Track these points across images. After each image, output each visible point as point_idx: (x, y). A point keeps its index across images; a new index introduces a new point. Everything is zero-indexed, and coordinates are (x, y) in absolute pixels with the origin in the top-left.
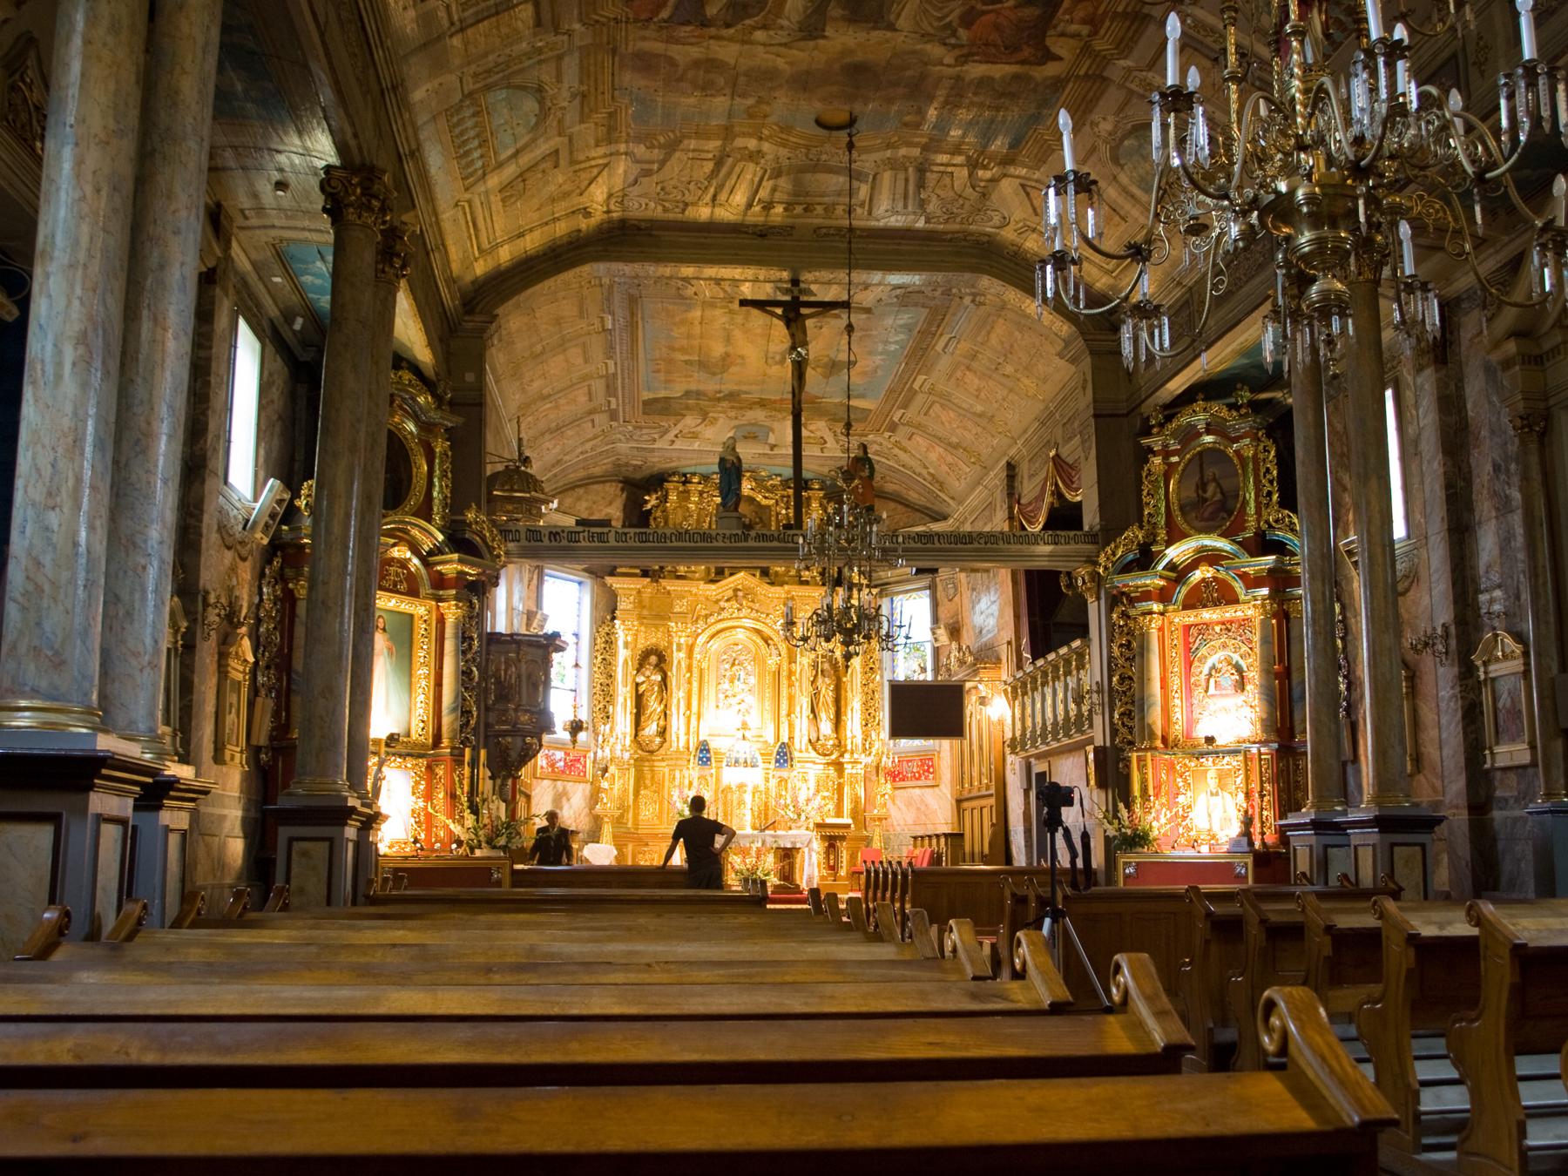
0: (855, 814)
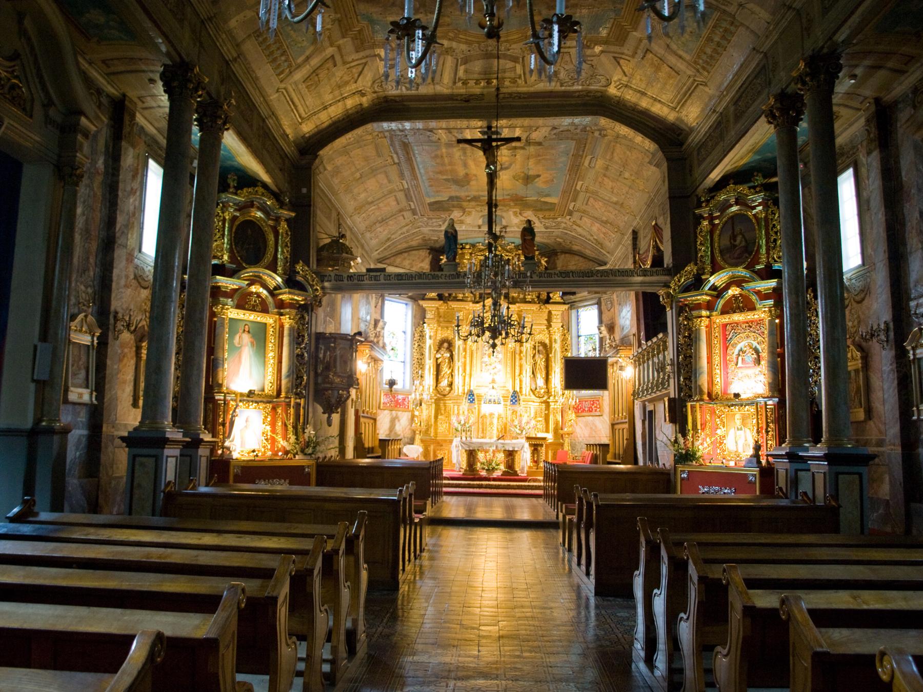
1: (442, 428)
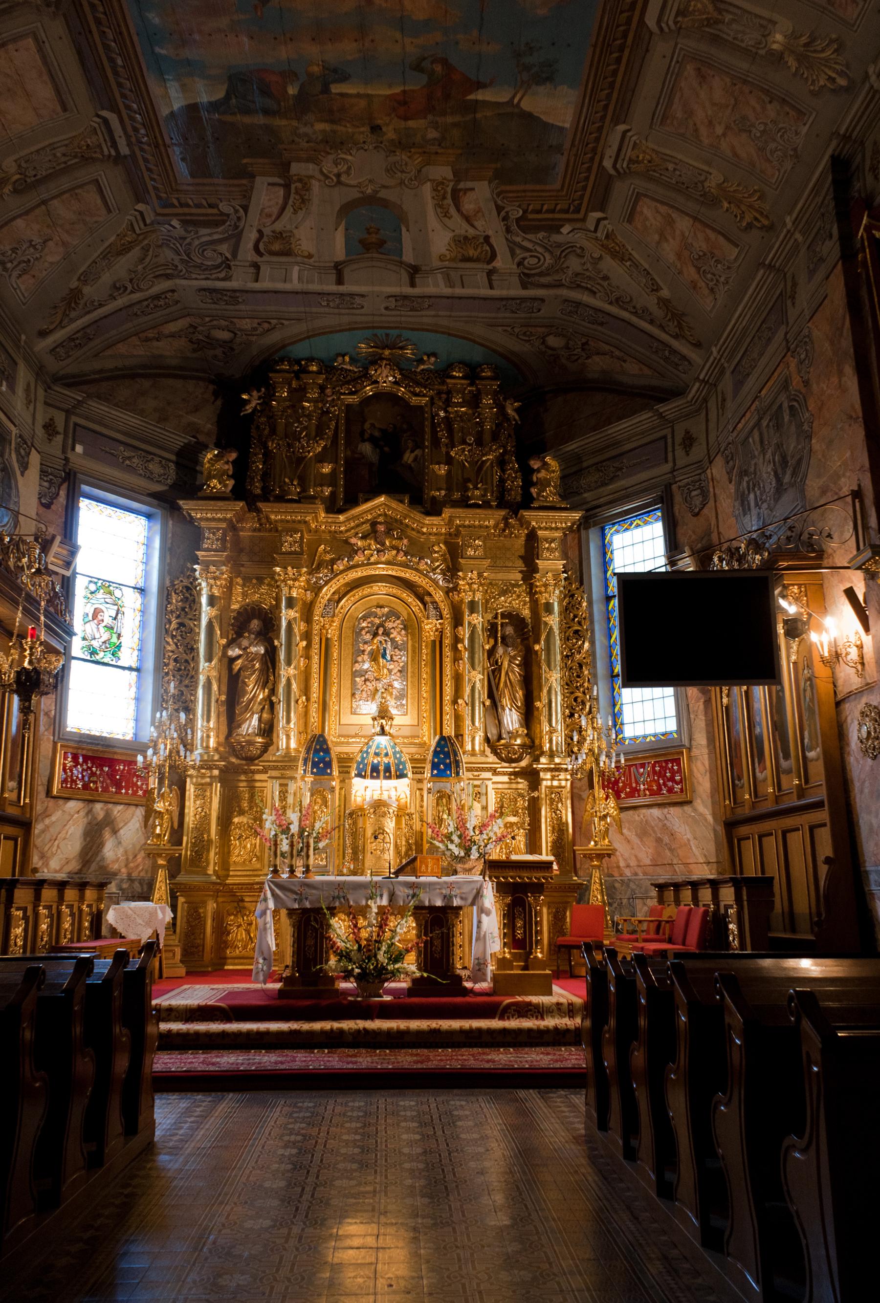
0: (558, 848)
1: (242, 850)
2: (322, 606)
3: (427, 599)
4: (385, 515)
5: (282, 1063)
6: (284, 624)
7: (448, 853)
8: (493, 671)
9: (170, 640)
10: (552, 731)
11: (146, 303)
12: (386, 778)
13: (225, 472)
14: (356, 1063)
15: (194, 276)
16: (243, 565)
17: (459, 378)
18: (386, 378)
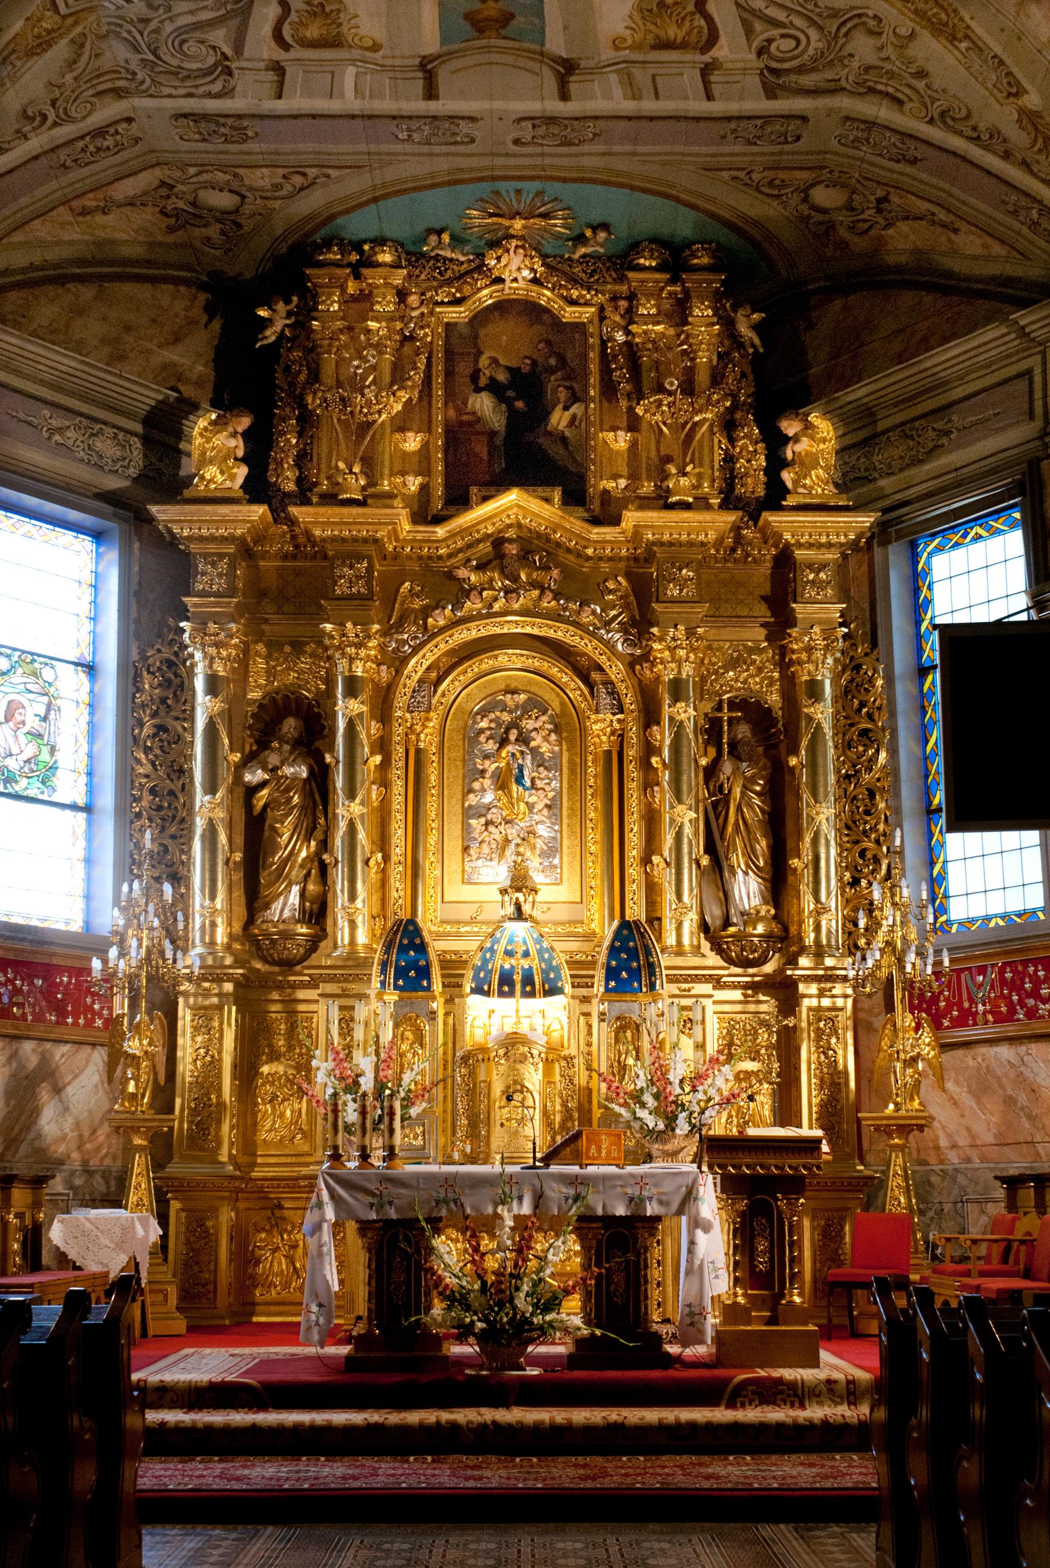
0: (831, 1114)
2: (408, 691)
3: (595, 676)
4: (519, 525)
5: (355, 1478)
6: (341, 724)
7: (636, 1125)
8: (715, 805)
9: (142, 756)
10: (820, 911)
11: (81, 144)
12: (526, 995)
13: (230, 453)
14: (480, 1478)
15: (167, 91)
16: (266, 621)
17: (650, 269)
18: (516, 271)
